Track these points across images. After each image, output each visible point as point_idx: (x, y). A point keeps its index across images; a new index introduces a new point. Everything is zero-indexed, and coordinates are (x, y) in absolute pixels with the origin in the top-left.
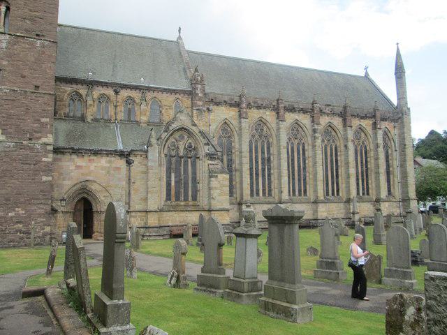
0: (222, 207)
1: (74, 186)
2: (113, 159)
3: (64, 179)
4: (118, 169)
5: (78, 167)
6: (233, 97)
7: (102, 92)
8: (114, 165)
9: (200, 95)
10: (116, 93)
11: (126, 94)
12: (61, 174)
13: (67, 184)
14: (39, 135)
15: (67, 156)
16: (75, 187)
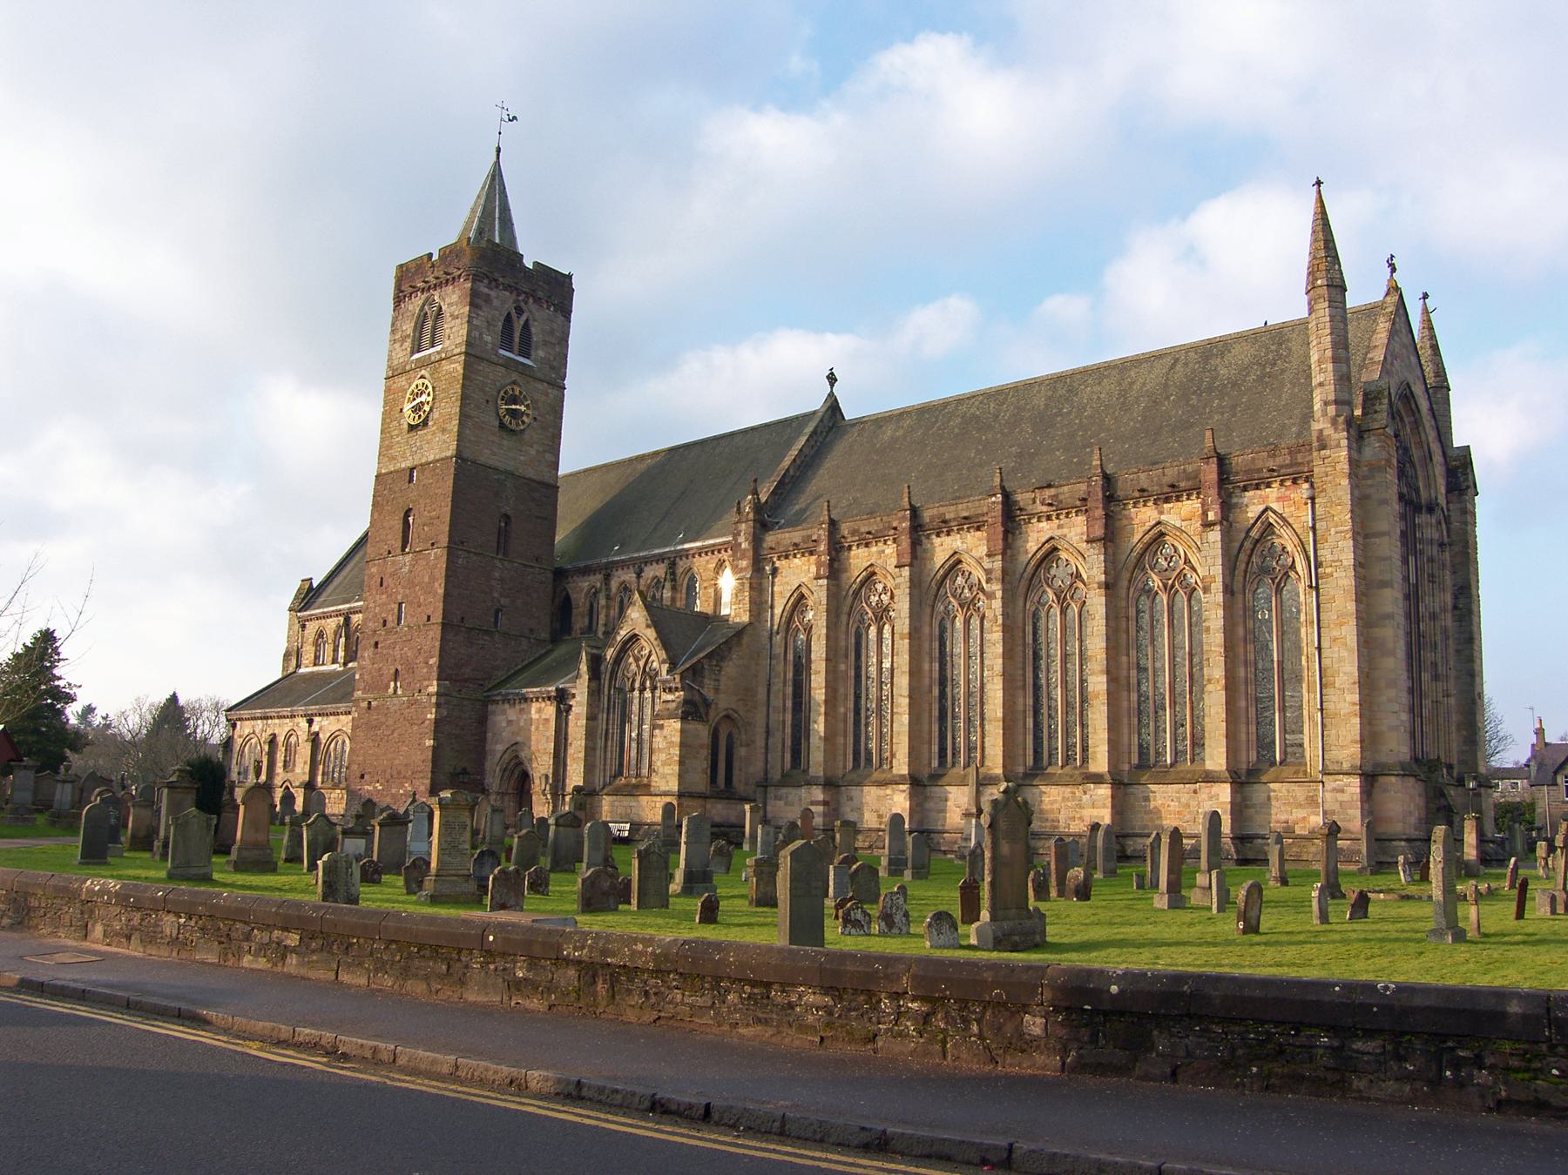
0: (667, 789)
1: (505, 752)
2: (543, 705)
3: (497, 743)
4: (547, 720)
5: (510, 722)
6: (809, 532)
7: (622, 579)
8: (544, 717)
9: (743, 546)
10: (639, 576)
11: (651, 574)
12: (494, 734)
13: (500, 748)
14: (426, 683)
15: (500, 707)
16: (506, 756)
